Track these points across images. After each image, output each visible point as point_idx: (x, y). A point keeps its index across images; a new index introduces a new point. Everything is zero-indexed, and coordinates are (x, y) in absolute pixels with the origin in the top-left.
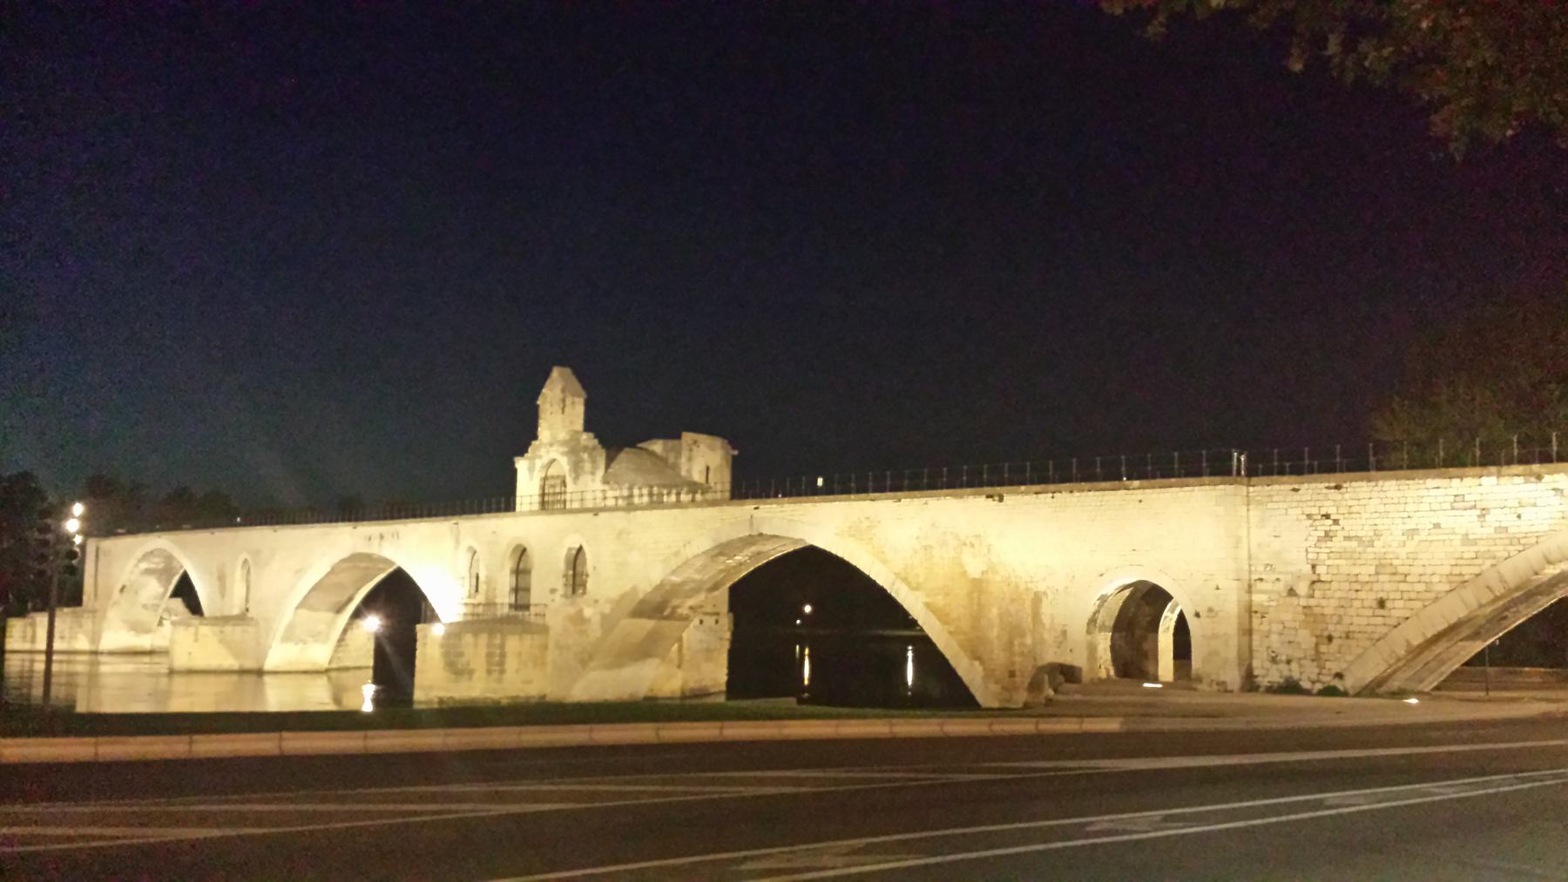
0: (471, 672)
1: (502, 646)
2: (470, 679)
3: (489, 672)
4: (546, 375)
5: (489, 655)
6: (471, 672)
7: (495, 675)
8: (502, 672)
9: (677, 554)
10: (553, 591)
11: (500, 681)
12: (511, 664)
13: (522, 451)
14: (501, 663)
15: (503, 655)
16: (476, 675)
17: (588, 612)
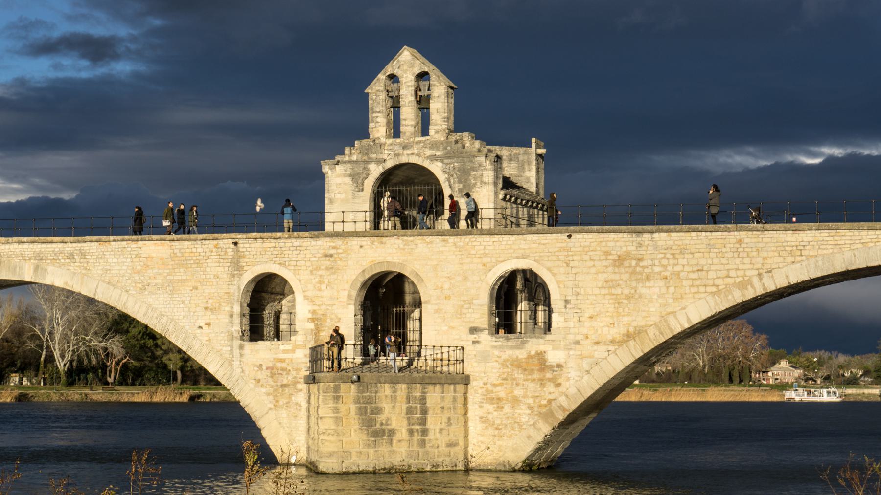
0: (392, 432)
1: (423, 399)
2: (391, 442)
3: (411, 432)
4: (392, 54)
5: (410, 411)
6: (392, 432)
7: (417, 437)
8: (425, 432)
9: (742, 286)
10: (473, 330)
11: (423, 443)
12: (433, 423)
13: (334, 152)
14: (423, 422)
15: (425, 412)
16: (398, 436)
17: (554, 356)
